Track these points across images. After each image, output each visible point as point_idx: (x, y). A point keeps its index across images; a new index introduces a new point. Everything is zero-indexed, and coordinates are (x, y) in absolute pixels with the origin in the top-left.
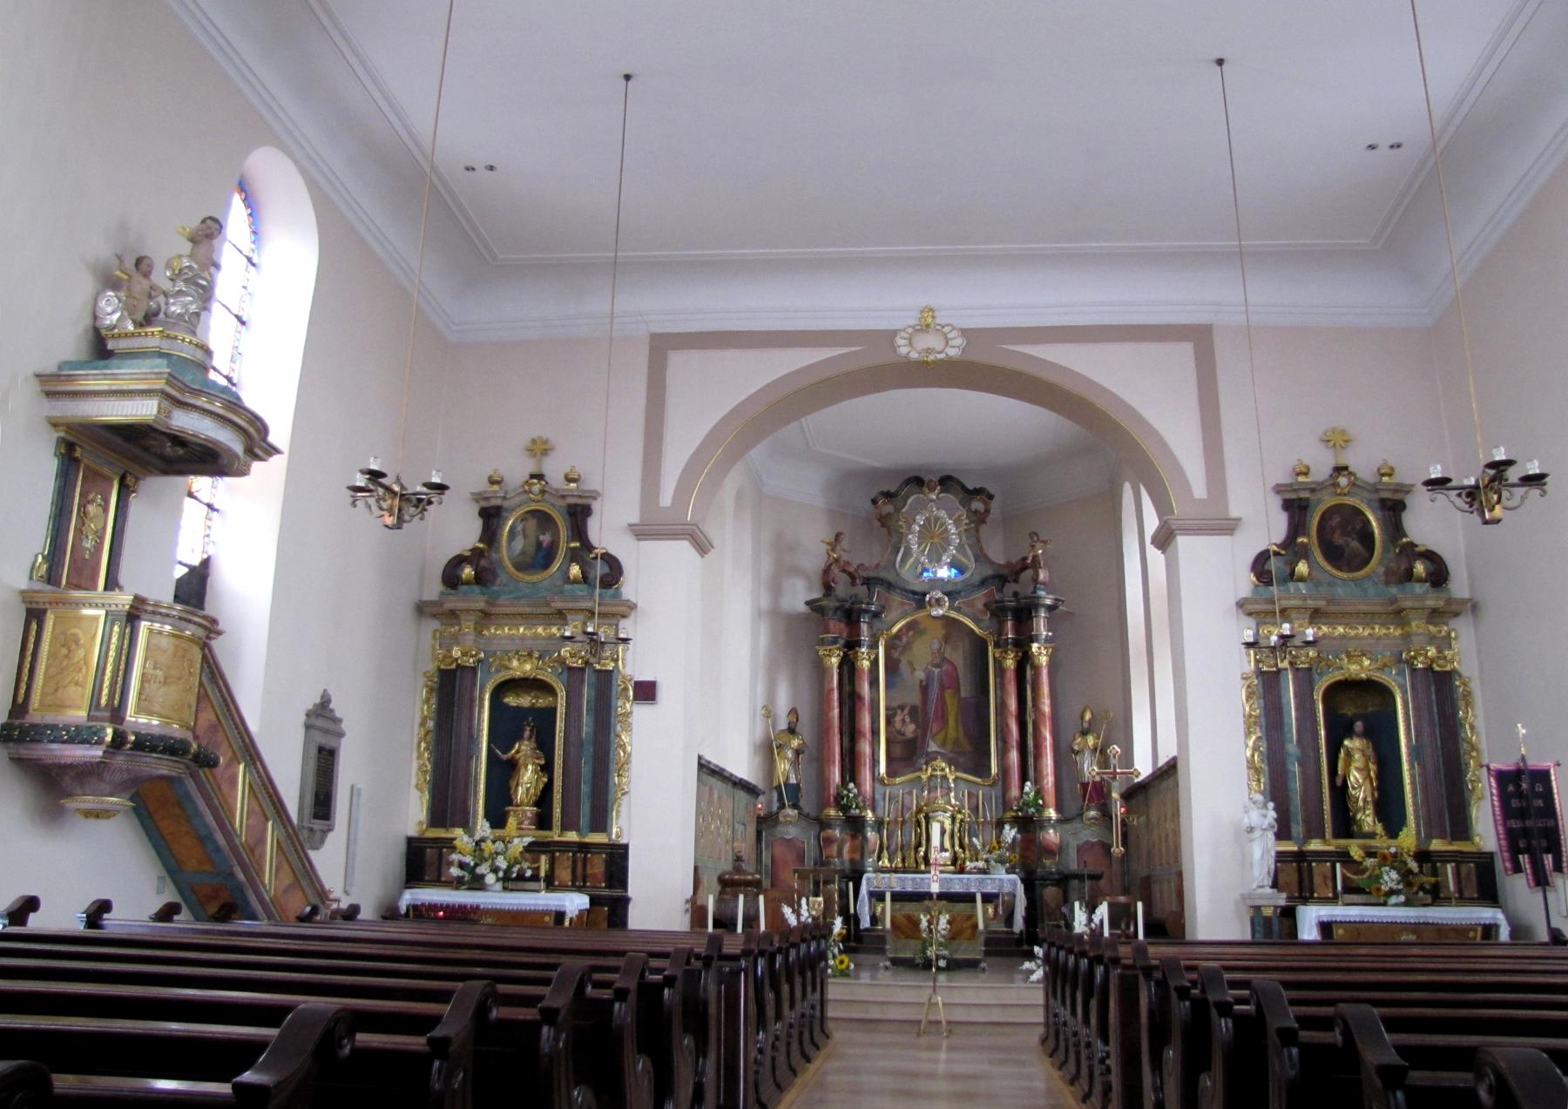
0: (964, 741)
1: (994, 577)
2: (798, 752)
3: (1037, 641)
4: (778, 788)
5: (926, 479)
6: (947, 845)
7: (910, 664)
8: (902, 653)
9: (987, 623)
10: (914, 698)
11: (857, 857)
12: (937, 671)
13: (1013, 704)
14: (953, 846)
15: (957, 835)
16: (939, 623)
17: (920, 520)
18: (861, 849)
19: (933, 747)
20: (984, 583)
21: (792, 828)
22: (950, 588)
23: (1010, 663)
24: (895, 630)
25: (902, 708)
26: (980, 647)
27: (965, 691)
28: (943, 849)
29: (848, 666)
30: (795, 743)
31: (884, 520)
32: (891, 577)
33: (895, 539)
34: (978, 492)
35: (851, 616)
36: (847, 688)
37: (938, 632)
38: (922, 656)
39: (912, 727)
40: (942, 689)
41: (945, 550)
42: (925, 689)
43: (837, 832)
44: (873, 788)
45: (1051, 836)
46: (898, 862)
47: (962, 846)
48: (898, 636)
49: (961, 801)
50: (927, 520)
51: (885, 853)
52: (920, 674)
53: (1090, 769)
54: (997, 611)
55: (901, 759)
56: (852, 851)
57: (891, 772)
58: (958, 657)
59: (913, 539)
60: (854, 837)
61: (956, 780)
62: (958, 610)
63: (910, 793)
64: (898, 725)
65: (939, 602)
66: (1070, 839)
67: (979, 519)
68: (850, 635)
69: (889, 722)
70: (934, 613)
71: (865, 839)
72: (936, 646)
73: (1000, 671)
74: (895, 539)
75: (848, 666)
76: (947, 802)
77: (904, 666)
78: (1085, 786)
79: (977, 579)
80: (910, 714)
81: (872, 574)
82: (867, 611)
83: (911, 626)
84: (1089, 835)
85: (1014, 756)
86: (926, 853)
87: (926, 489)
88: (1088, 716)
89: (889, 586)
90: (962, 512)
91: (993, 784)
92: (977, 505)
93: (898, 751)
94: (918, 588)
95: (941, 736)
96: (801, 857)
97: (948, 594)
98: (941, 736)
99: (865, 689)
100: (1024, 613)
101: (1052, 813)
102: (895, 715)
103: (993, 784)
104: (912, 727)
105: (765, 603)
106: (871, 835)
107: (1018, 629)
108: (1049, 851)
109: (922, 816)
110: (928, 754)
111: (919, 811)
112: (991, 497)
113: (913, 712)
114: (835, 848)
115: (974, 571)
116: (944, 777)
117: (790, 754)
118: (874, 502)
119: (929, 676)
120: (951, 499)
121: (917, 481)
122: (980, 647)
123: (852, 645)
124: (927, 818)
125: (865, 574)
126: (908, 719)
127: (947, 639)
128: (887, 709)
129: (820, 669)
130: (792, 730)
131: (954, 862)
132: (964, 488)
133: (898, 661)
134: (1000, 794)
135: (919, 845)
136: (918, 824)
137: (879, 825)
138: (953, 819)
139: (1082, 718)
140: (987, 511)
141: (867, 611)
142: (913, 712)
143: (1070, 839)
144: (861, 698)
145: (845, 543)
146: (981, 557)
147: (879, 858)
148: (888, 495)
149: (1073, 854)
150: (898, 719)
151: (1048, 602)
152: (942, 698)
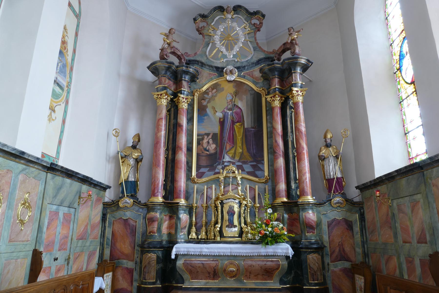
0: (246, 154)
1: (265, 58)
2: (138, 161)
3: (296, 87)
4: (121, 184)
5: (225, 8)
6: (236, 222)
7: (214, 108)
8: (209, 102)
9: (261, 84)
10: (217, 129)
11: (173, 232)
12: (230, 112)
13: (279, 128)
14: (240, 223)
15: (243, 215)
16: (231, 85)
17: (221, 28)
18: (174, 227)
19: (227, 158)
20: (259, 62)
21: (129, 211)
22: (238, 65)
23: (277, 103)
24: (204, 88)
25: (208, 135)
26: (257, 97)
27: (248, 122)
28: (231, 225)
29: (174, 107)
30: (136, 155)
31: (199, 31)
32: (204, 60)
33: (207, 40)
34: (256, 13)
35: (176, 77)
36: (172, 121)
37: (229, 89)
38: (219, 107)
39: (214, 146)
40: (233, 123)
41: (236, 44)
42: (222, 123)
43: (158, 215)
44: (187, 185)
45: (311, 215)
46: (203, 235)
47: (245, 223)
48: (206, 92)
49: (245, 193)
50: (225, 29)
51: (194, 229)
52: (219, 115)
53: (333, 170)
54: (266, 77)
55: (206, 167)
56: (170, 227)
57: (200, 175)
58: (242, 104)
59: (217, 38)
60: (171, 218)
61: (242, 178)
62: (244, 77)
63: (211, 188)
64: (205, 145)
65: (231, 72)
66: (322, 217)
67: (258, 28)
68: (176, 89)
69: (199, 143)
70: (228, 78)
71: (179, 219)
72: (230, 98)
73: (270, 110)
74: (207, 40)
75: (174, 107)
76: (237, 191)
77: (209, 111)
78: (330, 181)
79: (255, 60)
80: (212, 138)
81: (192, 58)
82: (187, 73)
83: (215, 87)
84: (335, 214)
85: (281, 162)
86: (221, 228)
87: (225, 13)
88: (329, 136)
89: (202, 65)
90: (246, 24)
91: (266, 183)
92: (255, 21)
93: (204, 162)
94: (219, 65)
95: (233, 151)
96: (133, 231)
97: (238, 68)
98: (233, 151)
99: (184, 121)
100: (285, 73)
101: (310, 199)
102: (203, 139)
103: (266, 183)
104: (214, 146)
105: (124, 70)
106: (184, 216)
107: (281, 82)
108: (310, 227)
109: (218, 202)
110: (224, 162)
111: (217, 199)
112: (264, 16)
113: (214, 137)
114: (156, 225)
115: (252, 56)
116: (235, 178)
117: (132, 162)
118: (195, 20)
119: (224, 117)
120: (241, 17)
121: (221, 9)
122: (257, 97)
123: (175, 95)
124: (222, 203)
125: (187, 58)
126: (211, 141)
127: (236, 94)
128: (198, 135)
129: (156, 109)
130: (134, 147)
131: (241, 235)
132: (247, 11)
133: (206, 107)
134: (270, 188)
135: (216, 223)
136: (216, 207)
137: (190, 210)
138: (240, 204)
139: (325, 137)
140: (261, 23)
141: (187, 73)
142: (214, 137)
143: (322, 217)
144: (181, 126)
145: (175, 37)
146: (258, 48)
147: (189, 233)
148: (204, 17)
149: (325, 227)
150: (205, 141)
151: (303, 61)
152: (232, 129)
